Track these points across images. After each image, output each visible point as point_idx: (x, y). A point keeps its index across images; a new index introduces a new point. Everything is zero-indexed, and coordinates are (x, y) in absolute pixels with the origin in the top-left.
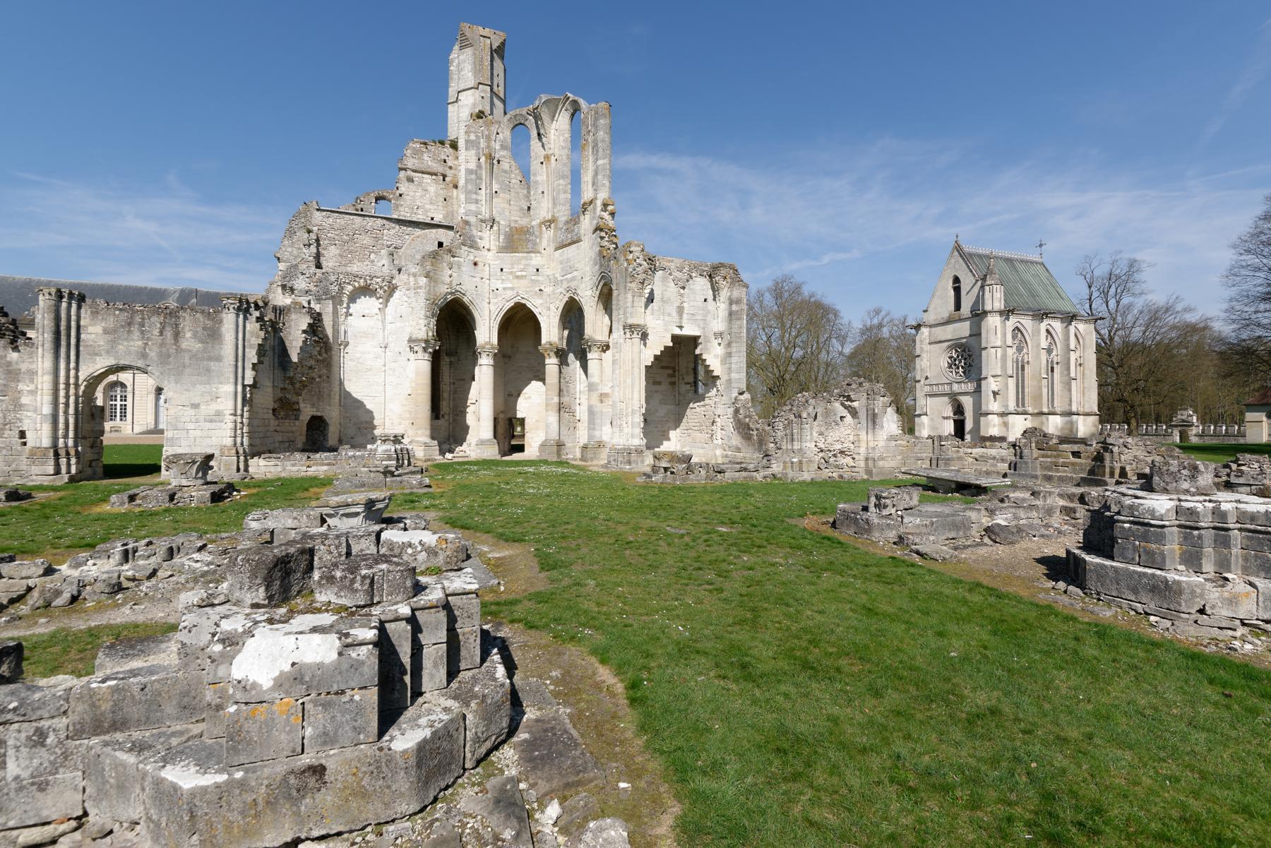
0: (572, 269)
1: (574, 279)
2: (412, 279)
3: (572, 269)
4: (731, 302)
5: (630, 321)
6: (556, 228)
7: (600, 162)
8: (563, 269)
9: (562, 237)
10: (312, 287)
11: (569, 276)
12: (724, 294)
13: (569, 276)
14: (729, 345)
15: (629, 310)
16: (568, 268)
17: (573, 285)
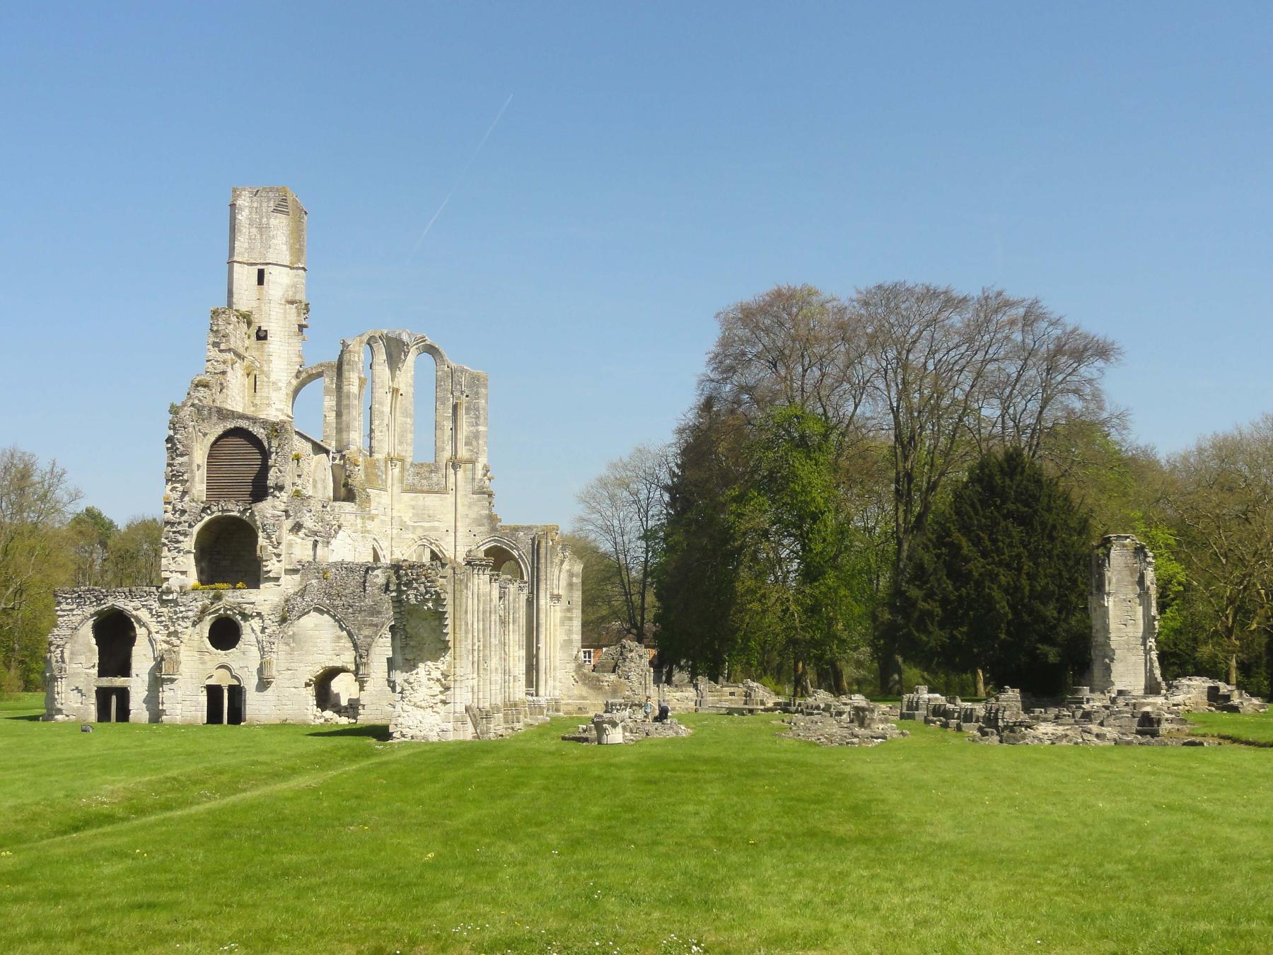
0: (431, 518)
1: (435, 529)
2: (359, 521)
3: (431, 518)
4: (571, 575)
5: (556, 592)
6: (403, 469)
7: (481, 428)
8: (414, 515)
9: (410, 479)
10: (318, 527)
11: (427, 525)
12: (566, 566)
13: (427, 525)
14: (569, 610)
15: (555, 582)
16: (422, 515)
17: (433, 535)
